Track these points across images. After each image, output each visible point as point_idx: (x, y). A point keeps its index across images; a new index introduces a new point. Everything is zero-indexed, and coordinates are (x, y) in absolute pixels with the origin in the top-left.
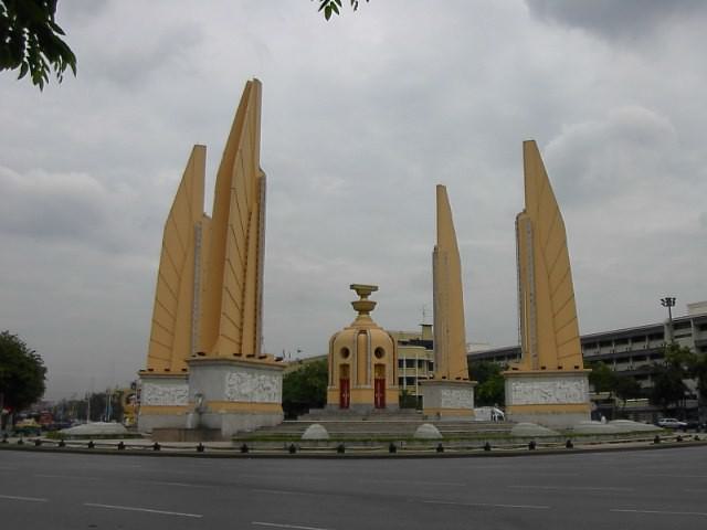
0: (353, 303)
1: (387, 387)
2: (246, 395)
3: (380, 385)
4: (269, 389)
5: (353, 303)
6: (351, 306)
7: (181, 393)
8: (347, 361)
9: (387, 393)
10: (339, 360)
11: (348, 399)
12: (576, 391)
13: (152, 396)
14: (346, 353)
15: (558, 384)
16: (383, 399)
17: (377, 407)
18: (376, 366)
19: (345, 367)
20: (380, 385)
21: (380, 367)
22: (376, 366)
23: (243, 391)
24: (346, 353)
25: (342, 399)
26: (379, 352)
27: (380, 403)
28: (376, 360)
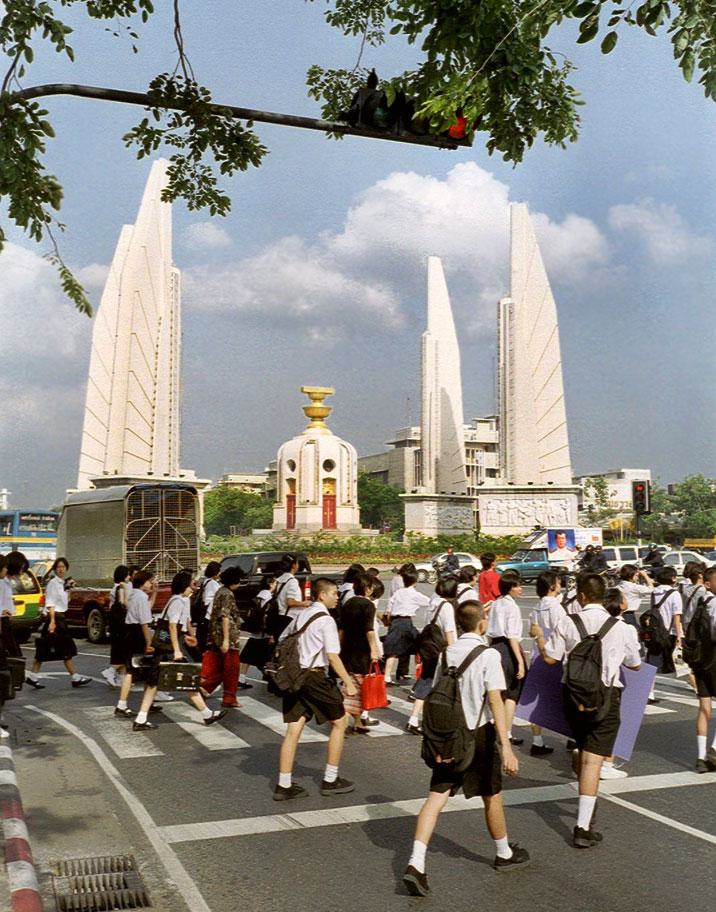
1: (338, 503)
3: (330, 502)
8: (294, 475)
9: (339, 511)
11: (295, 517)
14: (293, 466)
15: (539, 503)
16: (333, 518)
17: (325, 526)
18: (326, 480)
20: (330, 502)
24: (293, 466)
25: (289, 517)
26: (329, 465)
27: (330, 521)
28: (324, 474)
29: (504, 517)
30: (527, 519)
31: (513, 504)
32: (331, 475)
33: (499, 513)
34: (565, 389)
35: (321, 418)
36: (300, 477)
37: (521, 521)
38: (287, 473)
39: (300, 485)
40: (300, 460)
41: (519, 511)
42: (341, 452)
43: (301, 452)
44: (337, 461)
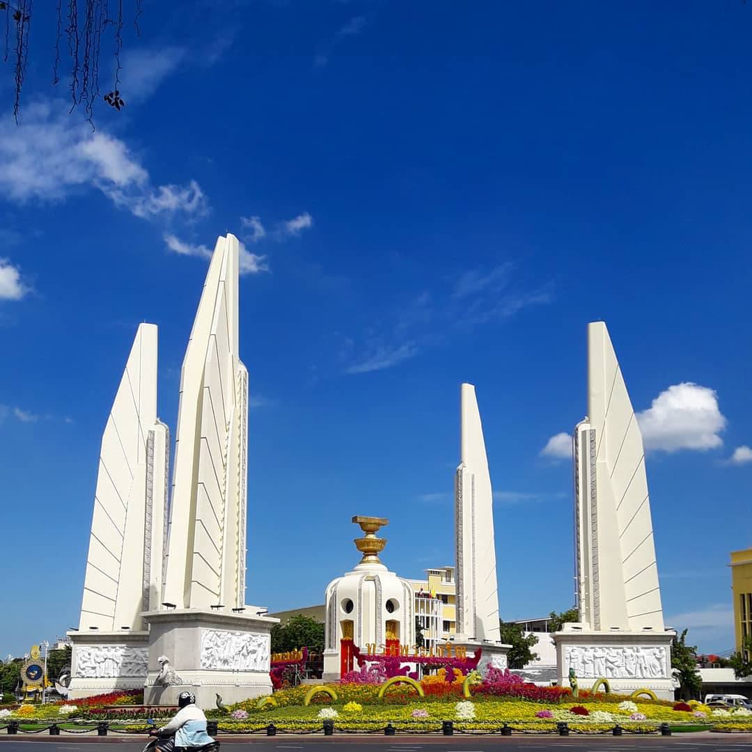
2: (225, 661)
4: (254, 652)
10: (342, 615)
12: (657, 663)
13: (88, 664)
14: (349, 606)
15: (629, 652)
18: (387, 622)
19: (348, 625)
21: (392, 626)
22: (387, 622)
23: (224, 655)
24: (349, 606)
28: (387, 616)
29: (590, 667)
30: (616, 670)
31: (599, 653)
32: (393, 616)
33: (584, 662)
34: (653, 528)
35: (374, 553)
36: (360, 618)
38: (342, 615)
39: (360, 628)
40: (360, 598)
41: (607, 660)
42: (405, 591)
43: (360, 590)
44: (400, 599)
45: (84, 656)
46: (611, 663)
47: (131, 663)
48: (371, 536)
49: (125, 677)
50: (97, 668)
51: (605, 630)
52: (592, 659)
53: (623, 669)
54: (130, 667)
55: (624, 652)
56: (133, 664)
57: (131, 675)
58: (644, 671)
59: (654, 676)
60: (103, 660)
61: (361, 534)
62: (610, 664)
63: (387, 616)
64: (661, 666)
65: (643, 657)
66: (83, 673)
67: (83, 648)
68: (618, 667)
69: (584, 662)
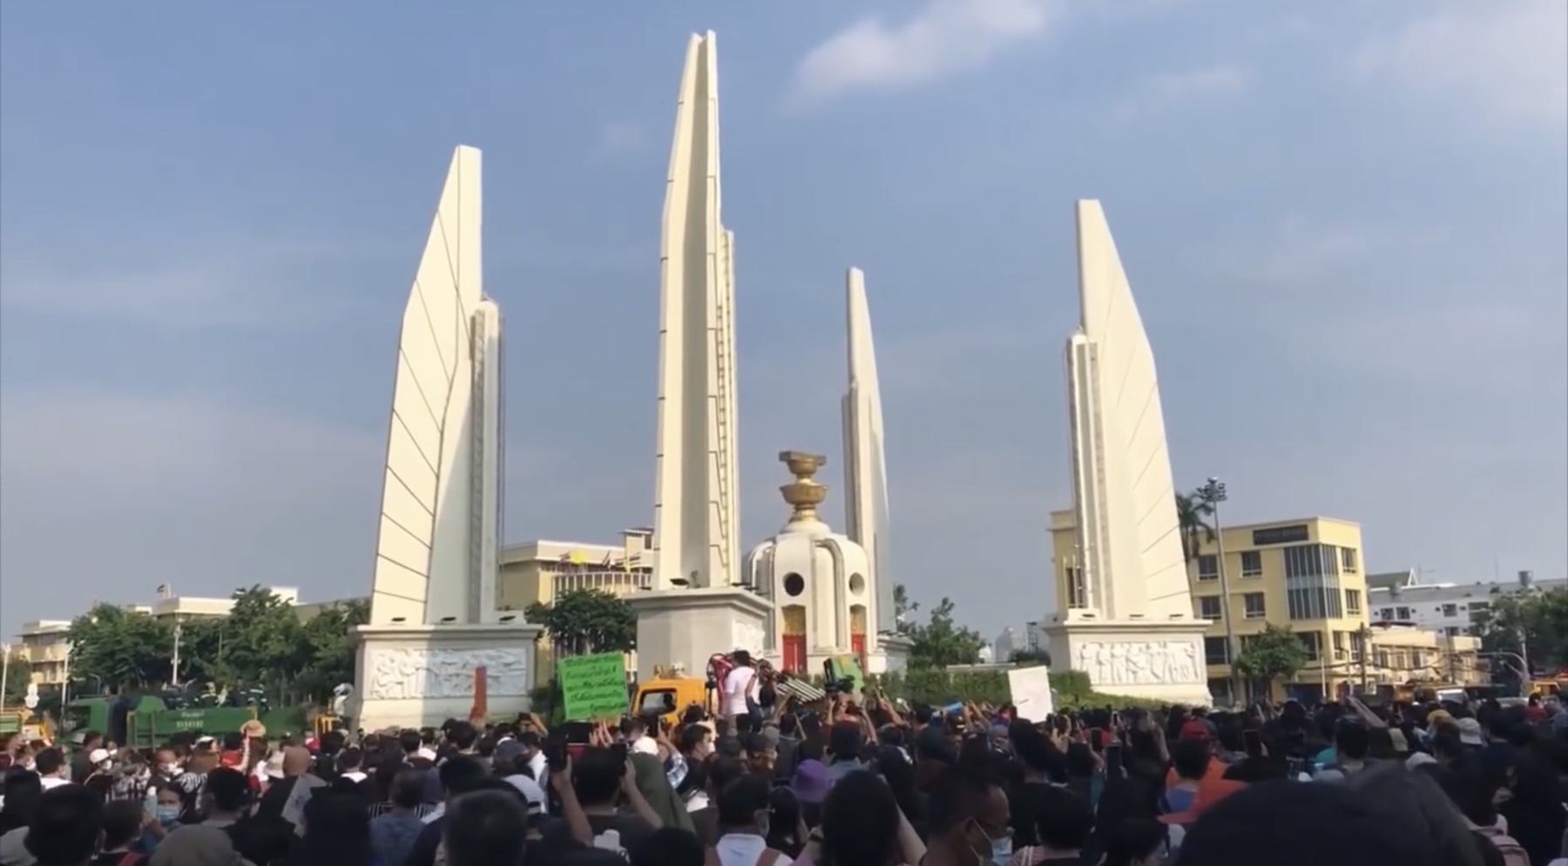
0: (783, 489)
5: (783, 489)
6: (780, 494)
7: (452, 670)
10: (783, 598)
24: (794, 584)
26: (856, 582)
30: (1140, 674)
37: (1131, 676)
45: (384, 665)
46: (1134, 664)
47: (457, 675)
48: (806, 481)
49: (448, 697)
50: (406, 685)
51: (1121, 619)
52: (1109, 658)
53: (1148, 673)
54: (455, 681)
55: (1148, 647)
56: (461, 678)
57: (458, 694)
58: (1174, 672)
59: (1185, 680)
60: (414, 670)
61: (790, 479)
62: (1132, 667)
63: (851, 599)
64: (1194, 666)
65: (1173, 656)
66: (383, 691)
67: (382, 652)
68: (1142, 669)
69: (1100, 663)
